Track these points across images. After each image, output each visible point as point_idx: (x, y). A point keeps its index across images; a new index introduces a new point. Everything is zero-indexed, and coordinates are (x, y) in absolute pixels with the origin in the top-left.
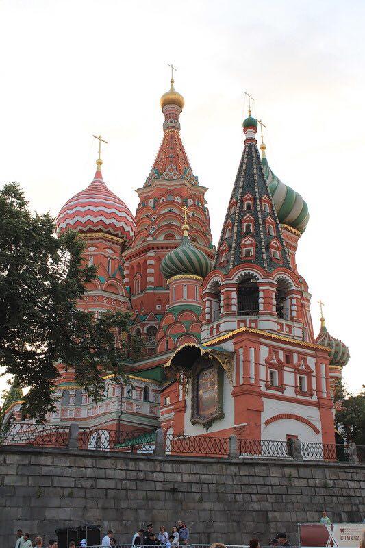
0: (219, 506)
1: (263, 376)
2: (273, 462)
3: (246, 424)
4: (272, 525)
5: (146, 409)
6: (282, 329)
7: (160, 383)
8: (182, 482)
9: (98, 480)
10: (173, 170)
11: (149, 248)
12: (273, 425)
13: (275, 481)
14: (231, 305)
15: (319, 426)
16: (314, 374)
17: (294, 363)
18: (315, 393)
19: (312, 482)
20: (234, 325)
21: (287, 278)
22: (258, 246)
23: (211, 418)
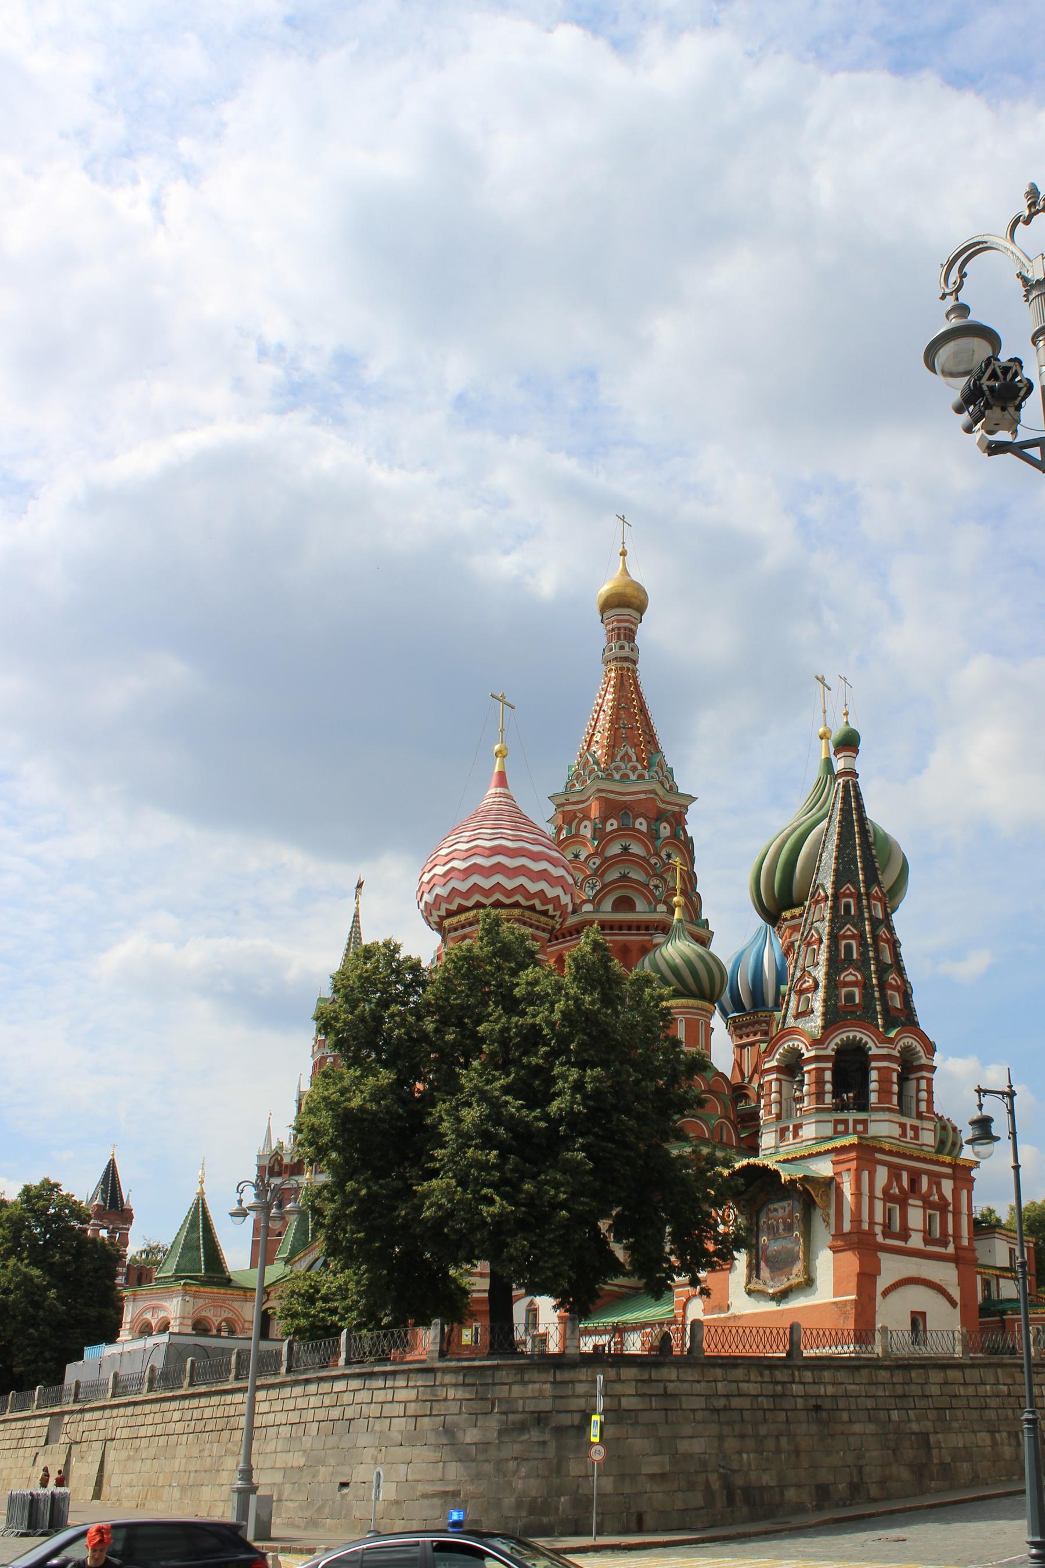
0: (871, 1428)
1: (879, 1217)
2: (933, 1362)
4: (935, 1452)
6: (904, 1134)
8: (826, 1396)
9: (732, 1399)
10: (630, 760)
12: (893, 1296)
13: (935, 1390)
15: (956, 1293)
16: (951, 1208)
17: (923, 1191)
18: (951, 1239)
19: (981, 1390)
21: (919, 1048)
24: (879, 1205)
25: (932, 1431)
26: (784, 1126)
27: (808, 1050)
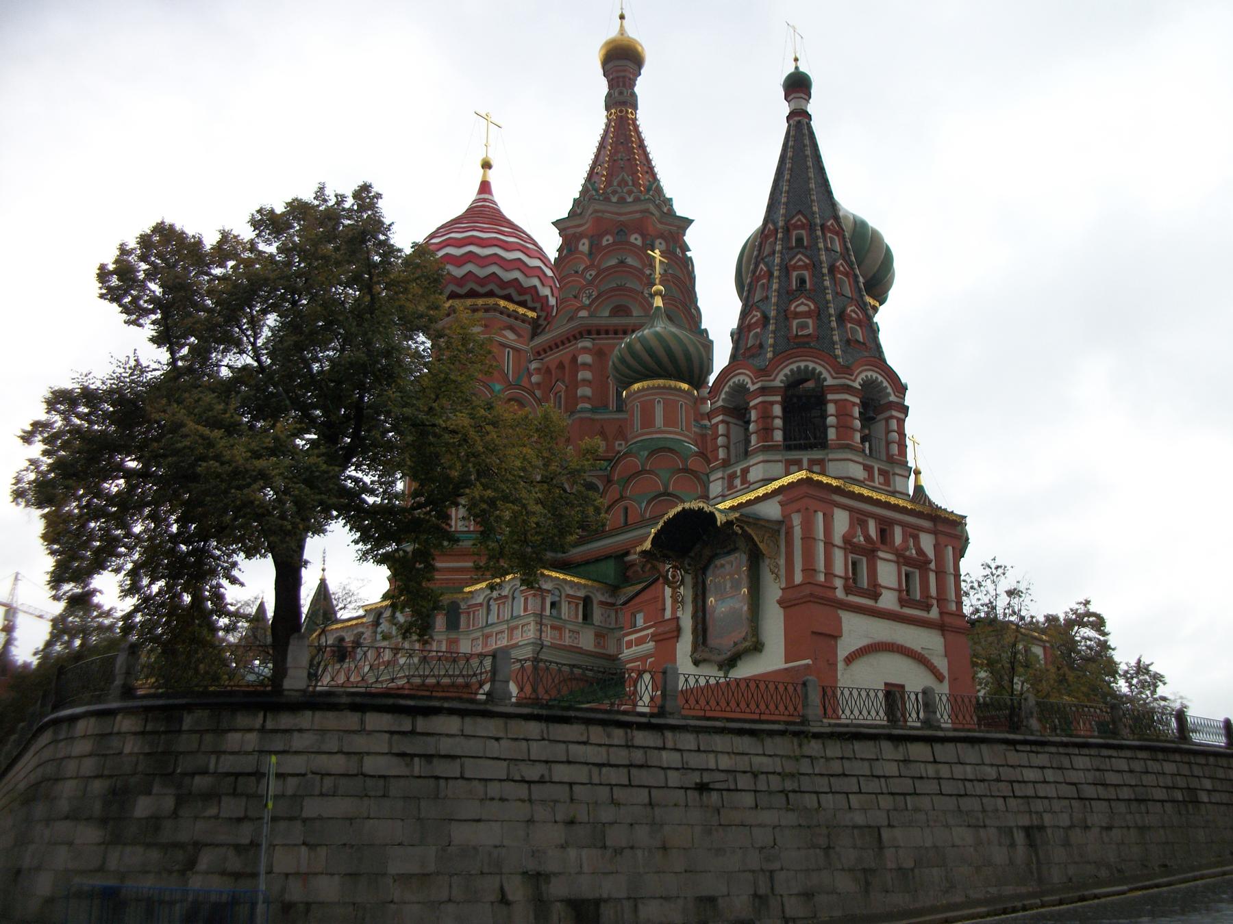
0: (790, 819)
1: (839, 567)
3: (808, 661)
4: (889, 853)
5: (587, 641)
6: (871, 478)
7: (614, 589)
8: (718, 770)
10: (626, 184)
11: (580, 333)
14: (773, 430)
15: (942, 664)
16: (933, 566)
17: (896, 544)
18: (935, 602)
19: (958, 771)
20: (780, 468)
22: (819, 314)
23: (734, 650)
24: (839, 556)
25: (886, 823)
26: (731, 471)
27: (753, 383)
